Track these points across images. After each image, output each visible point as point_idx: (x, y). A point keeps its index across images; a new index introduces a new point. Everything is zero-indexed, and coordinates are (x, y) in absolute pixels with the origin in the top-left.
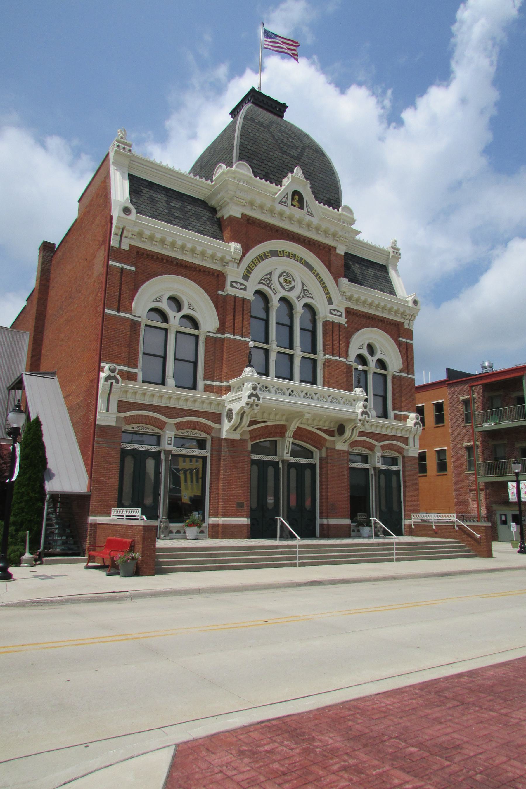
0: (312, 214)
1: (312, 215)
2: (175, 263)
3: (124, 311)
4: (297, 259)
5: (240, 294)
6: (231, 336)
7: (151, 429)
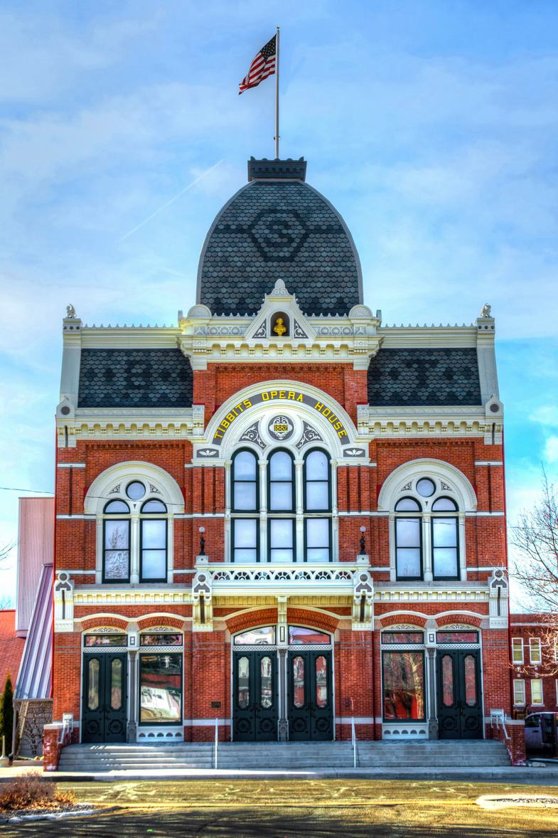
0: (304, 334)
1: (304, 336)
2: (129, 446)
3: (76, 513)
4: (291, 397)
5: (209, 463)
6: (199, 515)
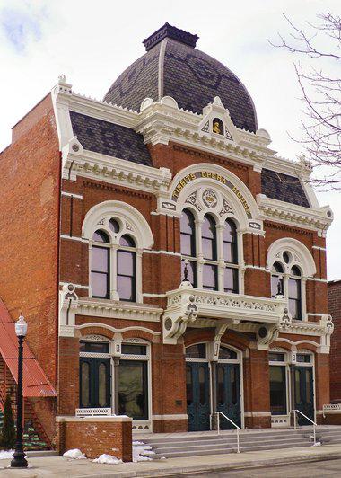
3: (75, 236)
5: (171, 214)
6: (165, 252)
7: (100, 339)
